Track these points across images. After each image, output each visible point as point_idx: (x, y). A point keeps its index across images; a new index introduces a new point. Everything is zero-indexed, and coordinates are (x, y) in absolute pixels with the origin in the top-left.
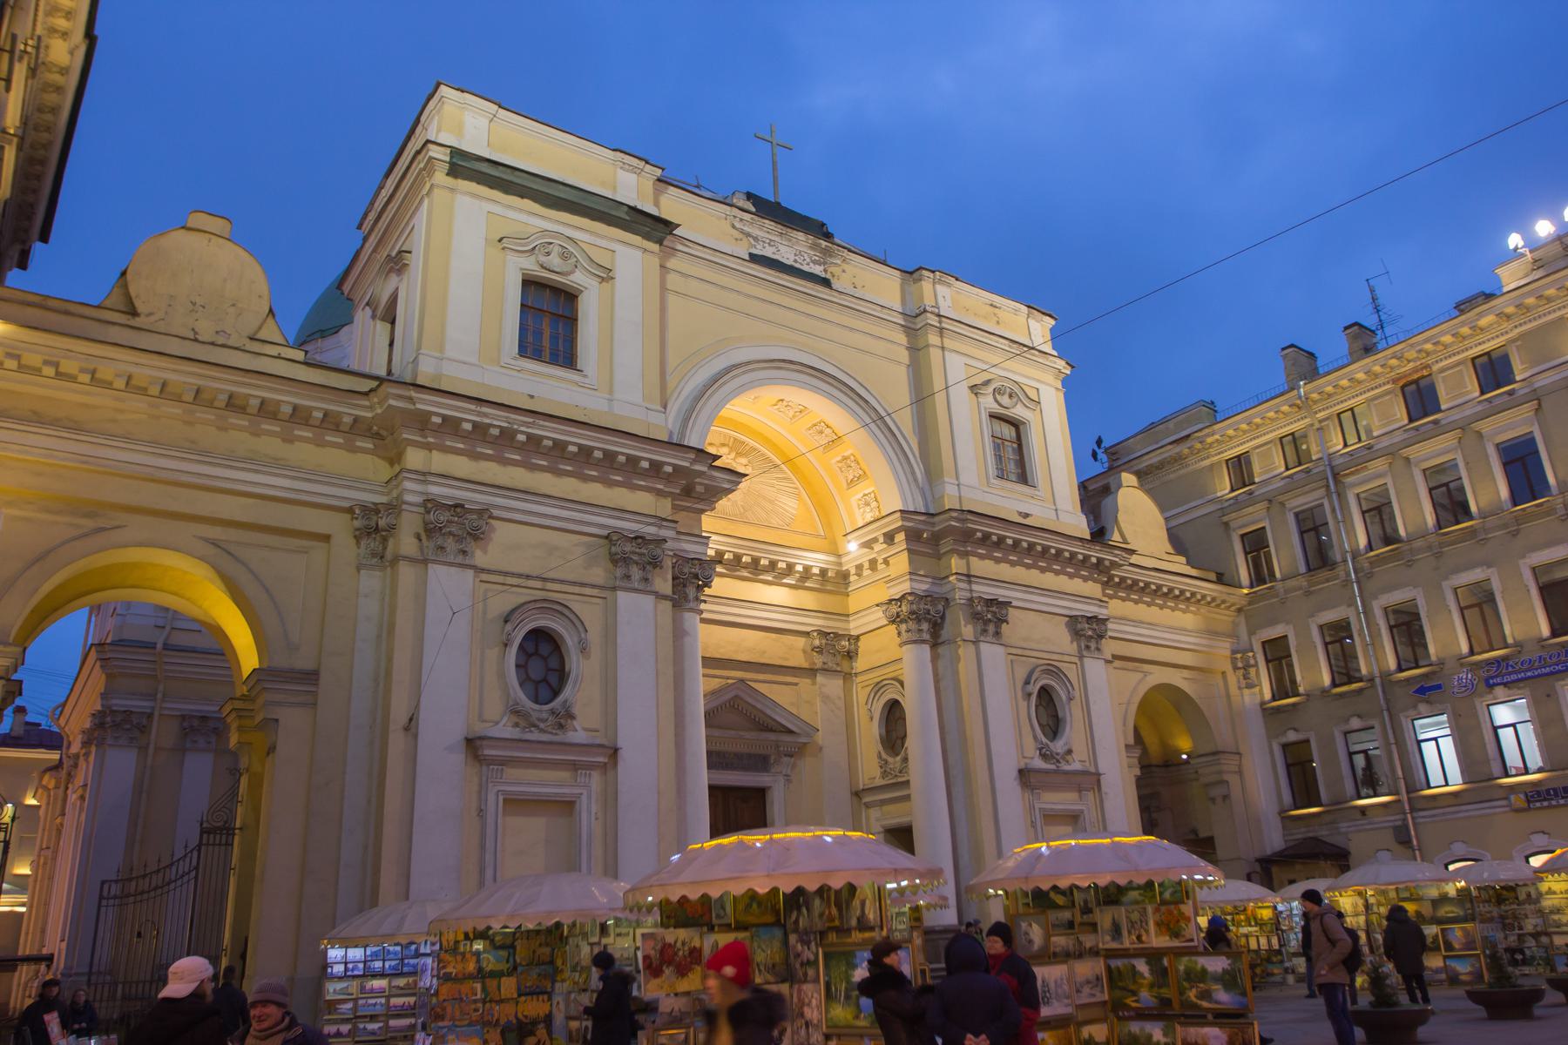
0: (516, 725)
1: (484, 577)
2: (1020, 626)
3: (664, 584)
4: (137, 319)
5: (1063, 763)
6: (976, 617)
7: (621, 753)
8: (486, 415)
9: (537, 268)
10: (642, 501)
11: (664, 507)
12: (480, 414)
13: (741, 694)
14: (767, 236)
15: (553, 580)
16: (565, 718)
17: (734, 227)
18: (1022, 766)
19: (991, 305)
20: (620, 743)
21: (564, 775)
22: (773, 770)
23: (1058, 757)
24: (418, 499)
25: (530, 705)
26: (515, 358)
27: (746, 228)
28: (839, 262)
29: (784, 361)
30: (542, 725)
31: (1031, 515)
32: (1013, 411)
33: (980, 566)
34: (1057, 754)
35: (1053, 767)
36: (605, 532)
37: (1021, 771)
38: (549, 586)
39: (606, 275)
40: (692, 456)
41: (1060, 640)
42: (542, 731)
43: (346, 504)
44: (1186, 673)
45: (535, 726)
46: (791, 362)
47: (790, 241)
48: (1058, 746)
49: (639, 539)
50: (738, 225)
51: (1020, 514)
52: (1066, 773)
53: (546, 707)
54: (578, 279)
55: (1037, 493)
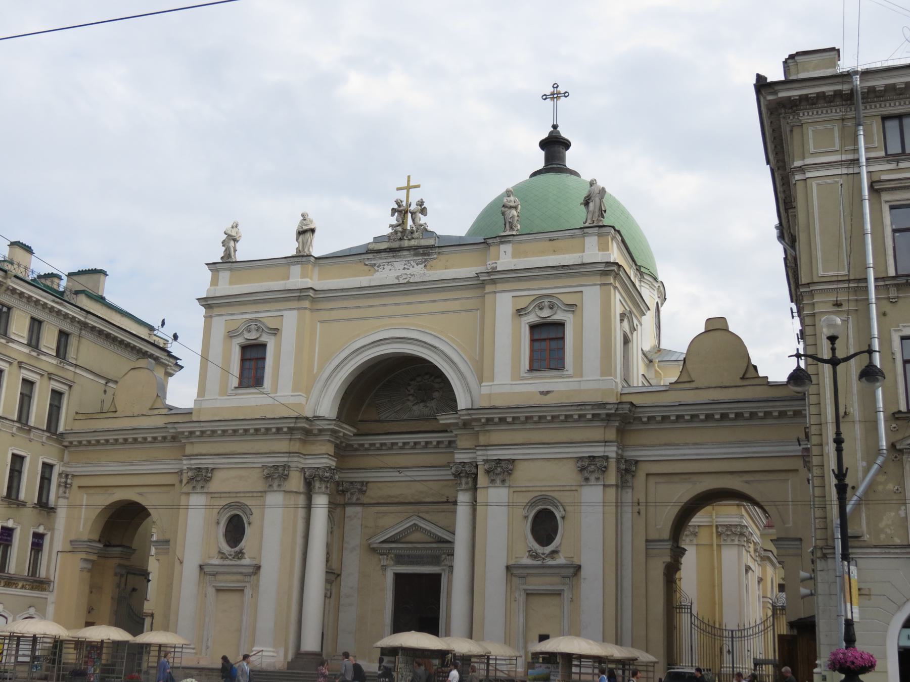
0: (222, 558)
1: (213, 495)
2: (523, 475)
3: (296, 482)
4: (117, 413)
5: (548, 559)
6: (488, 472)
7: (262, 570)
8: (203, 427)
9: (245, 341)
10: (283, 445)
11: (296, 446)
12: (201, 427)
13: (417, 522)
14: (385, 261)
15: (240, 492)
16: (240, 555)
17: (366, 265)
18: (511, 562)
19: (550, 240)
20: (261, 564)
21: (239, 577)
22: (443, 564)
23: (543, 556)
24: (185, 467)
25: (226, 548)
26: (233, 390)
27: (373, 262)
28: (435, 256)
29: (381, 340)
30: (230, 557)
31: (553, 391)
32: (552, 318)
33: (497, 437)
34: (543, 554)
35: (539, 563)
36: (260, 465)
37: (508, 568)
38: (238, 495)
39: (275, 331)
40: (294, 420)
41: (567, 474)
42: (231, 560)
43: (176, 471)
44: (747, 477)
45: (228, 558)
46: (385, 339)
47: (401, 258)
48: (548, 549)
49: (276, 467)
50: (367, 263)
51: (542, 393)
52: (551, 567)
53: (233, 549)
54: (264, 338)
55: (565, 373)
